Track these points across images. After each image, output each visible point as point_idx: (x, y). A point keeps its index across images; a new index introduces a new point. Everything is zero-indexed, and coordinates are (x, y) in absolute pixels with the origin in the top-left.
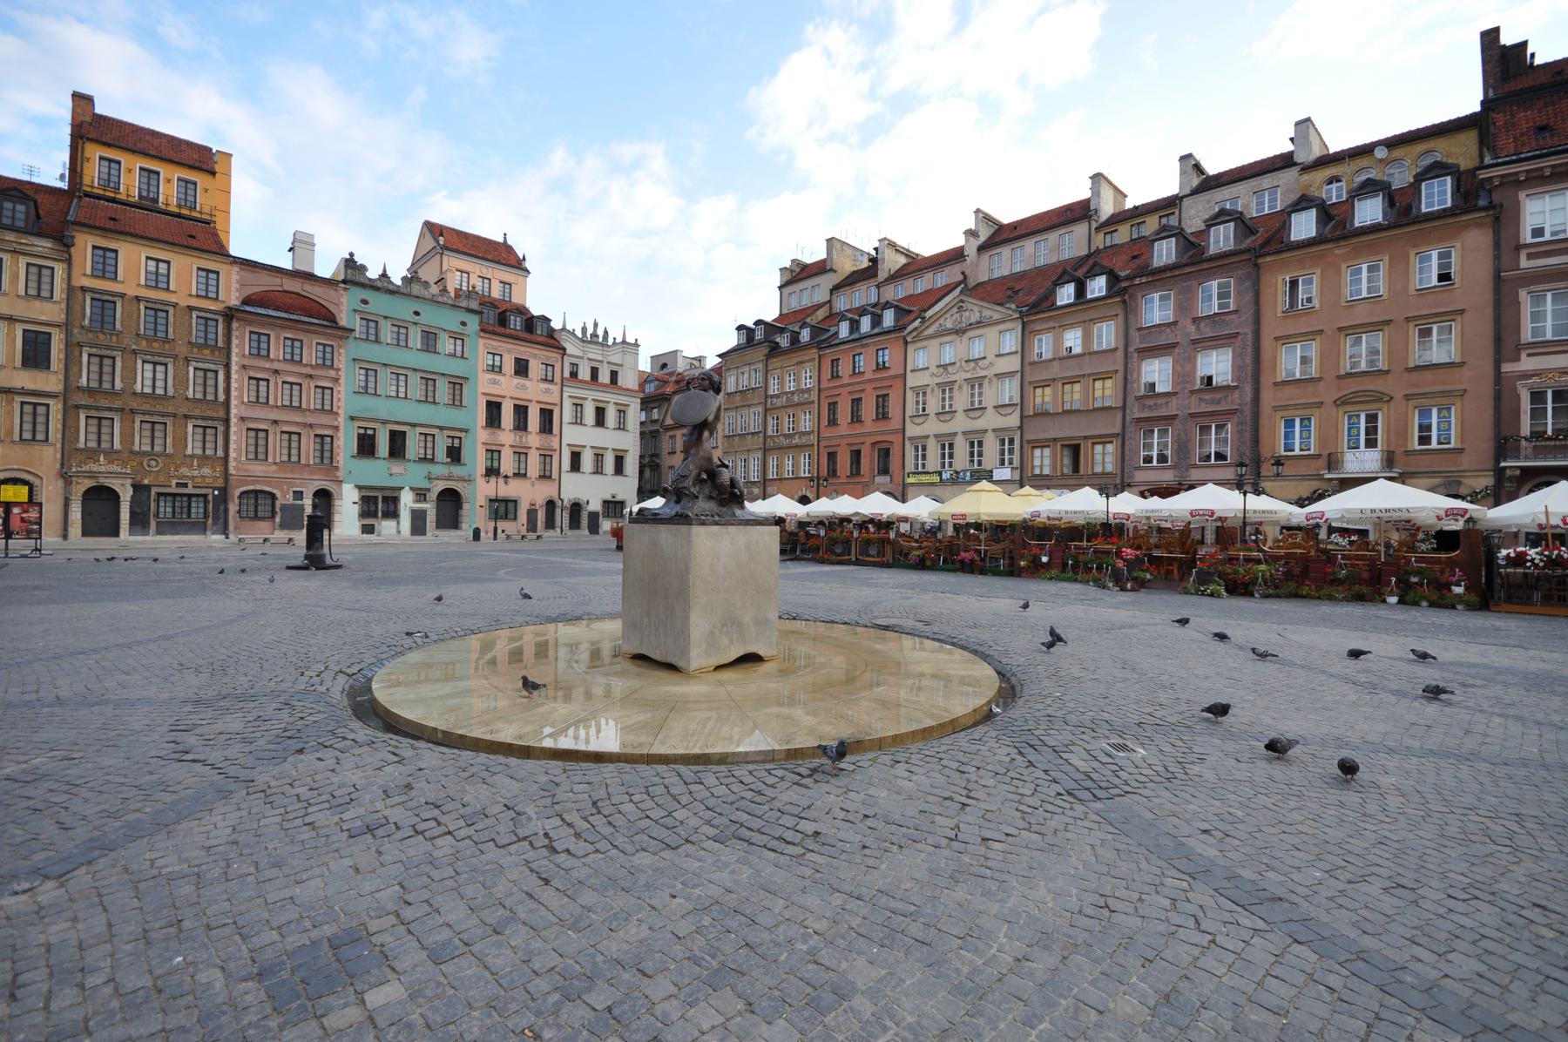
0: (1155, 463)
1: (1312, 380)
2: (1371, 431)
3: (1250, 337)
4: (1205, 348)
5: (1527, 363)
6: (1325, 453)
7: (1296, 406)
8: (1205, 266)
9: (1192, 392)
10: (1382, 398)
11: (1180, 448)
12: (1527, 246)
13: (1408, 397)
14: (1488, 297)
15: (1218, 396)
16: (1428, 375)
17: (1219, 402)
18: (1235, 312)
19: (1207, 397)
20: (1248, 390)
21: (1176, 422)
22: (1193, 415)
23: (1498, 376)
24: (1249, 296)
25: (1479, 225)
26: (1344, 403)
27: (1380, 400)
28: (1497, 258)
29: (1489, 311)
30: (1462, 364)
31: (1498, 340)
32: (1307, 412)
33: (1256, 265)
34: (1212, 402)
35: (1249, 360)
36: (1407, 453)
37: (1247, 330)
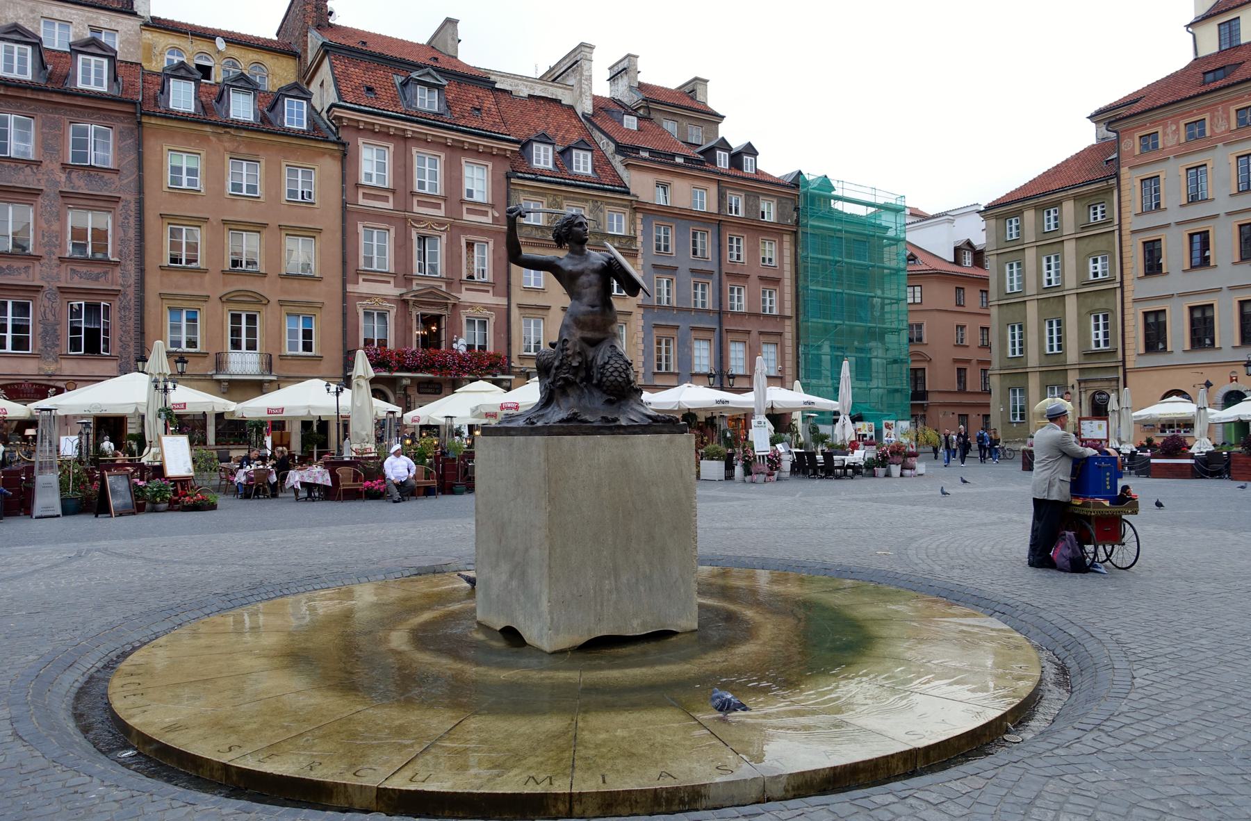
0: (9, 349)
1: (198, 270)
2: (251, 332)
3: (133, 206)
4: (77, 207)
5: (363, 287)
6: (212, 352)
7: (184, 297)
8: (79, 101)
9: (62, 260)
10: (261, 300)
11: (46, 332)
12: (363, 186)
13: (282, 303)
14: (338, 221)
15: (96, 270)
16: (296, 284)
17: (97, 279)
18: (116, 171)
19: (84, 269)
20: (131, 267)
21: (40, 296)
22: (63, 290)
23: (345, 295)
24: (132, 156)
25: (331, 155)
26: (229, 301)
27: (259, 302)
28: (343, 190)
29: (339, 235)
30: (320, 279)
31: (344, 262)
32: (193, 305)
33: (140, 123)
34: (89, 277)
35: (132, 233)
36: (282, 357)
37: (129, 197)
